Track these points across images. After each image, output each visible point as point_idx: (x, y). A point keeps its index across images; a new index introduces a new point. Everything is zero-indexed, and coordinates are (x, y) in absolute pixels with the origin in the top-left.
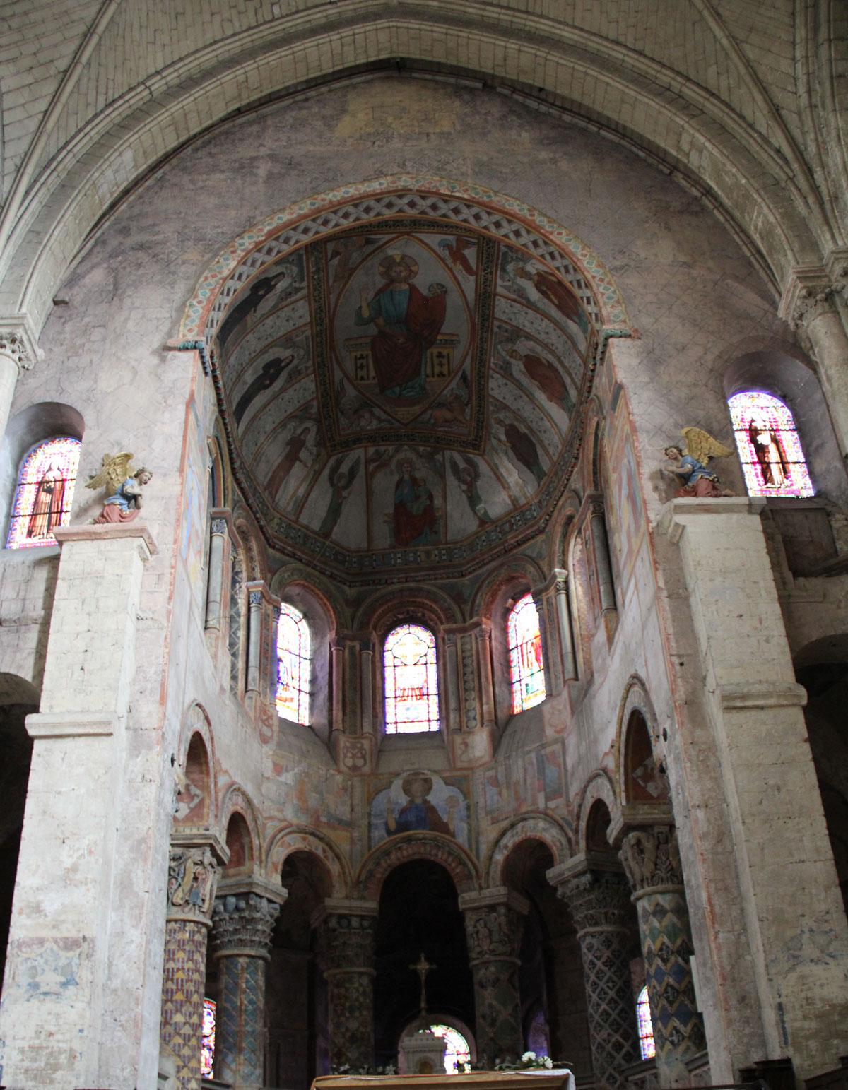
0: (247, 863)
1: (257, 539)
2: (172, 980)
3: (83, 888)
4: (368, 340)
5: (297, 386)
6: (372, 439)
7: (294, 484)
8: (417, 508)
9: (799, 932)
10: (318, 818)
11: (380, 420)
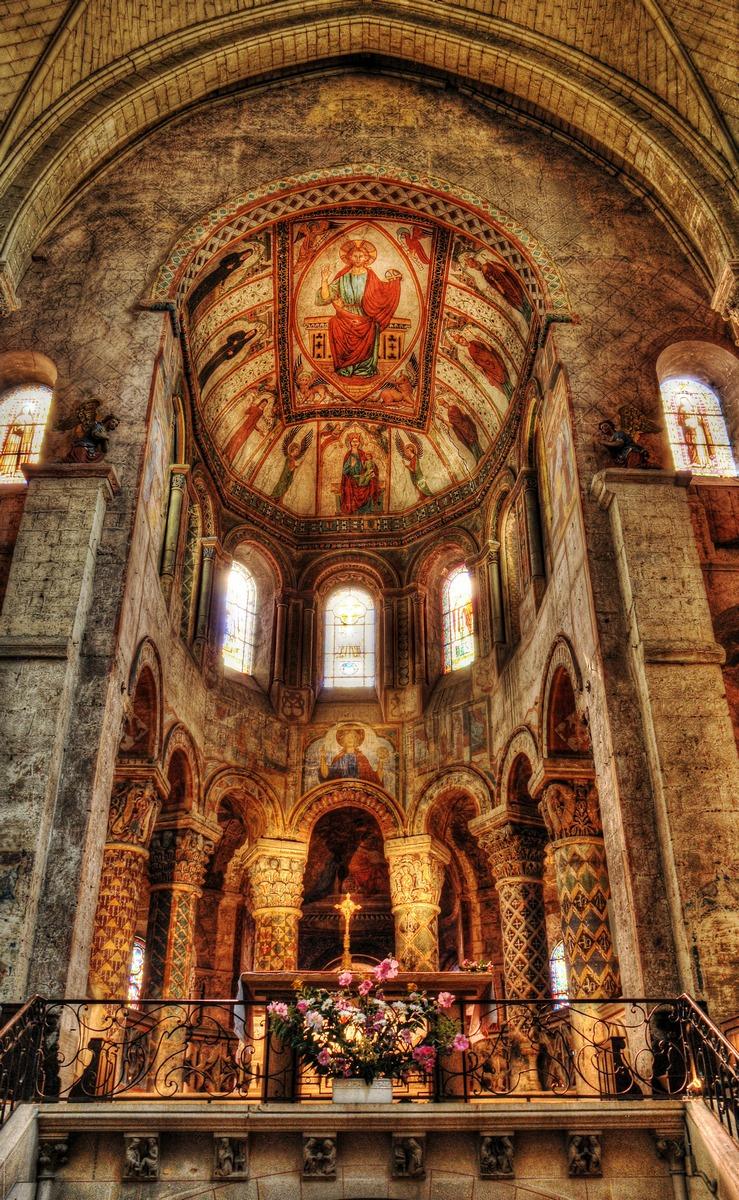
0: (188, 800)
1: (213, 498)
2: (106, 907)
3: (27, 804)
4: (327, 320)
5: (258, 359)
6: (325, 413)
8: (363, 479)
9: (714, 878)
10: (255, 762)
11: (334, 397)
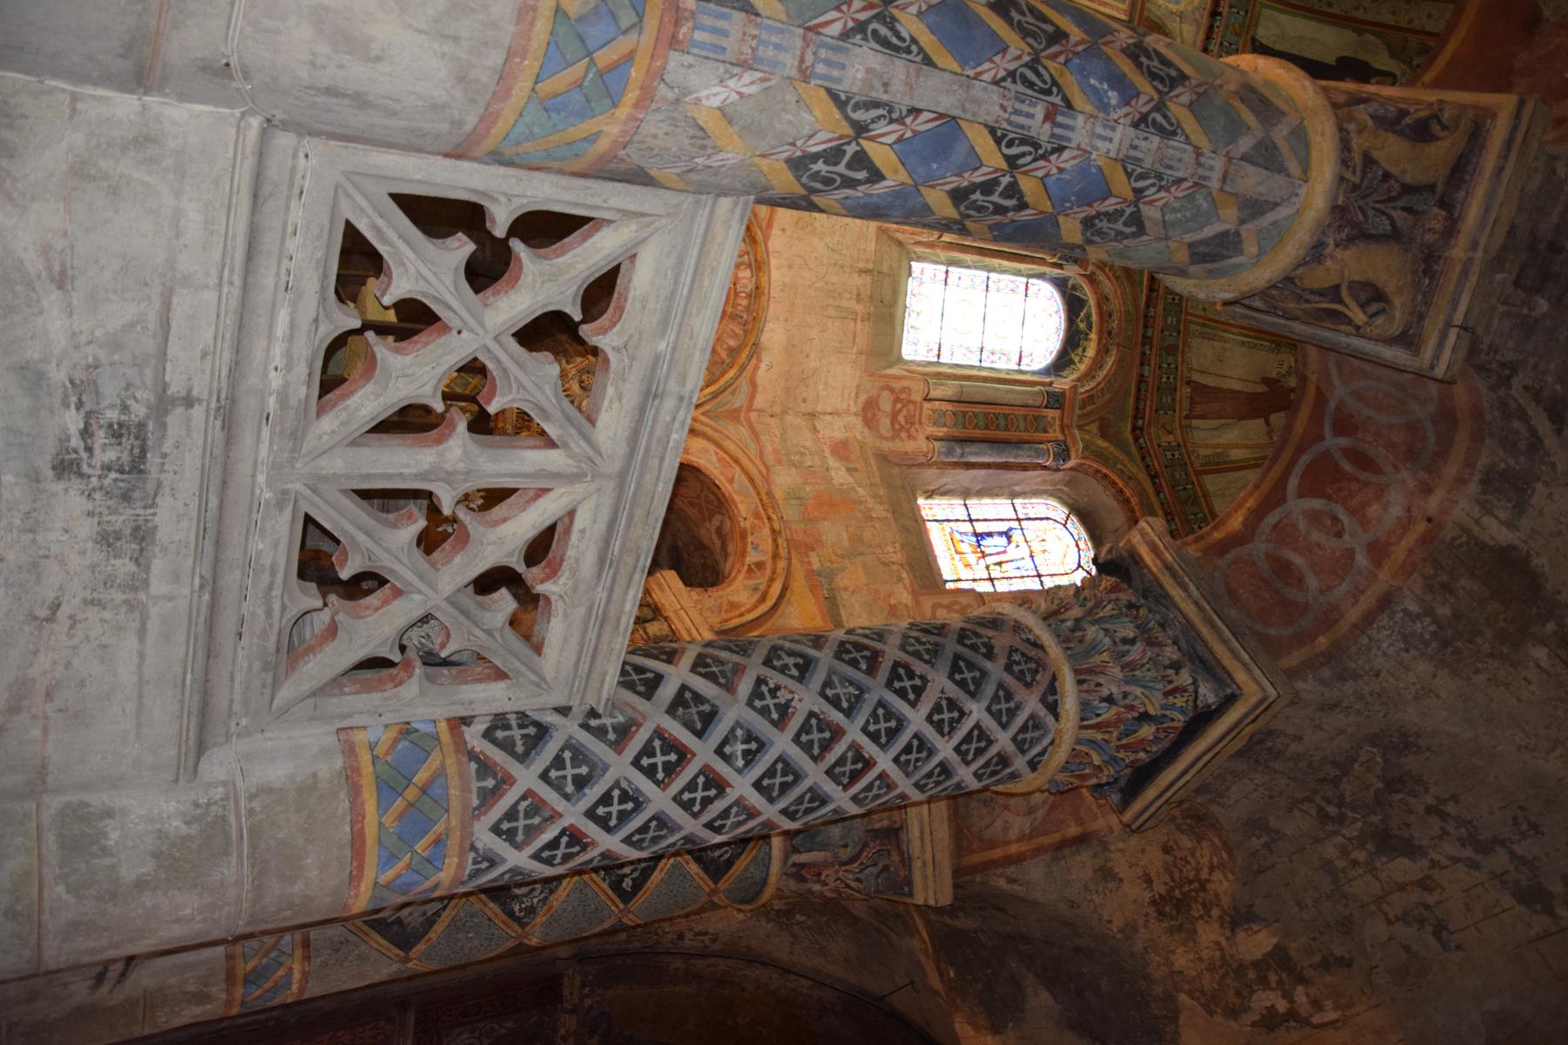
1: (1119, 362)
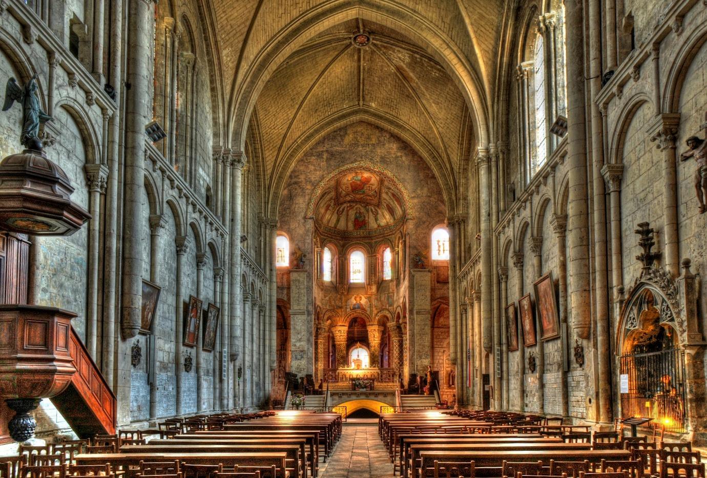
7: (327, 216)
8: (361, 220)
